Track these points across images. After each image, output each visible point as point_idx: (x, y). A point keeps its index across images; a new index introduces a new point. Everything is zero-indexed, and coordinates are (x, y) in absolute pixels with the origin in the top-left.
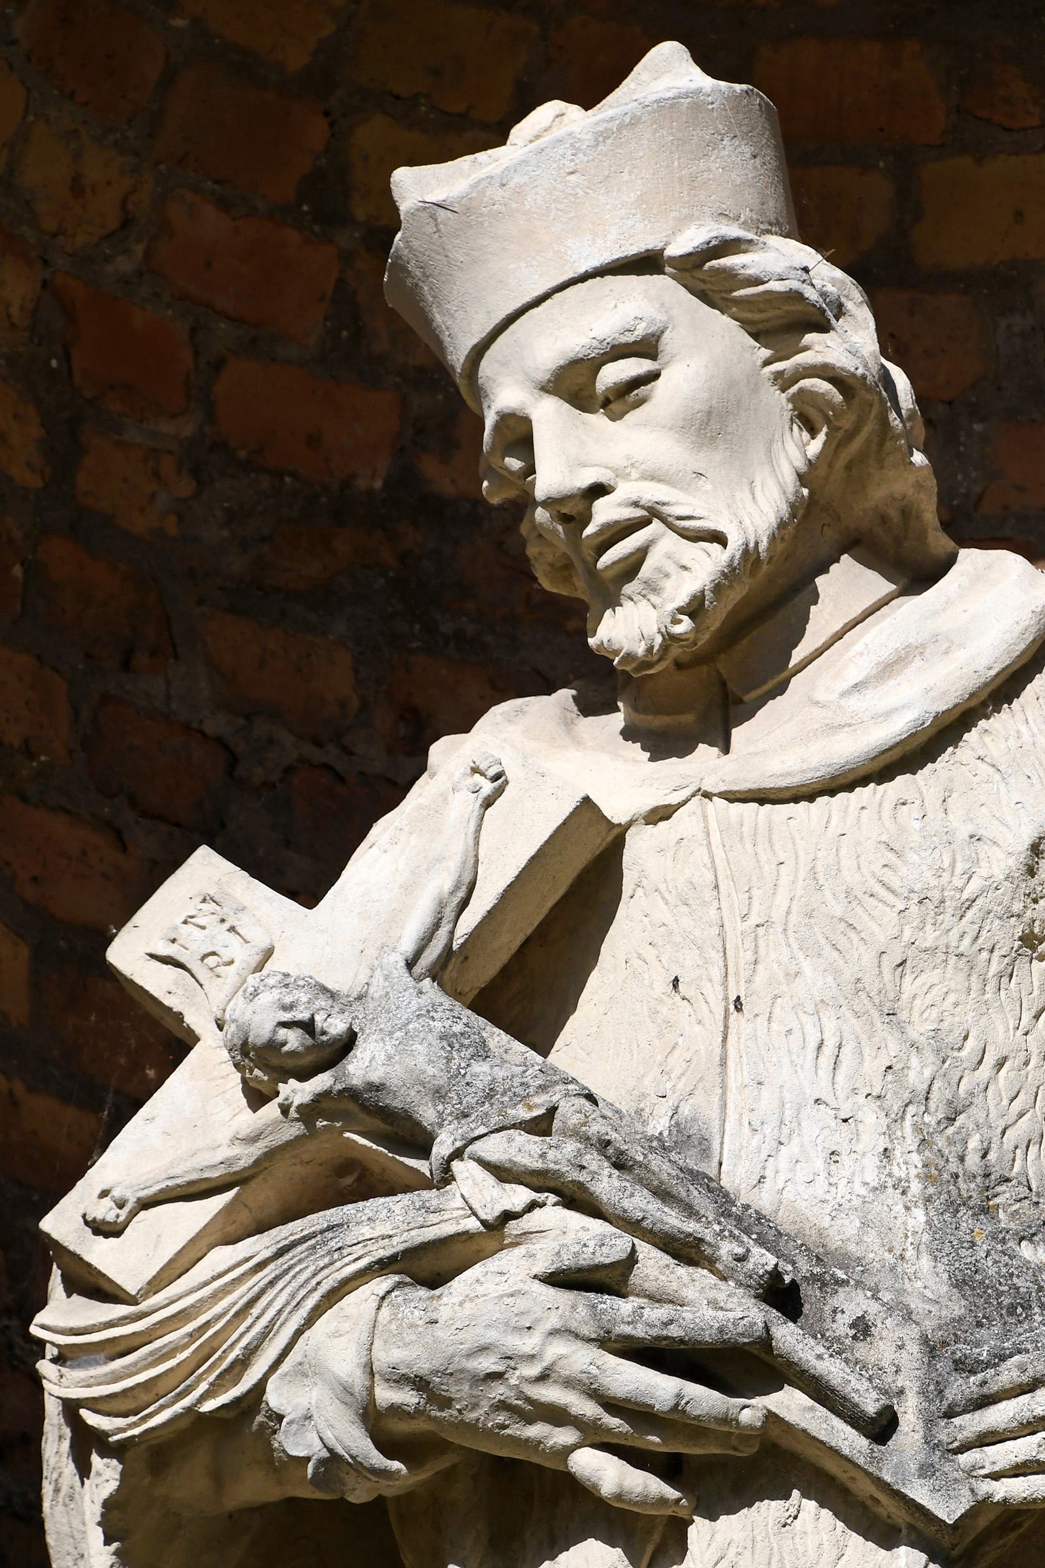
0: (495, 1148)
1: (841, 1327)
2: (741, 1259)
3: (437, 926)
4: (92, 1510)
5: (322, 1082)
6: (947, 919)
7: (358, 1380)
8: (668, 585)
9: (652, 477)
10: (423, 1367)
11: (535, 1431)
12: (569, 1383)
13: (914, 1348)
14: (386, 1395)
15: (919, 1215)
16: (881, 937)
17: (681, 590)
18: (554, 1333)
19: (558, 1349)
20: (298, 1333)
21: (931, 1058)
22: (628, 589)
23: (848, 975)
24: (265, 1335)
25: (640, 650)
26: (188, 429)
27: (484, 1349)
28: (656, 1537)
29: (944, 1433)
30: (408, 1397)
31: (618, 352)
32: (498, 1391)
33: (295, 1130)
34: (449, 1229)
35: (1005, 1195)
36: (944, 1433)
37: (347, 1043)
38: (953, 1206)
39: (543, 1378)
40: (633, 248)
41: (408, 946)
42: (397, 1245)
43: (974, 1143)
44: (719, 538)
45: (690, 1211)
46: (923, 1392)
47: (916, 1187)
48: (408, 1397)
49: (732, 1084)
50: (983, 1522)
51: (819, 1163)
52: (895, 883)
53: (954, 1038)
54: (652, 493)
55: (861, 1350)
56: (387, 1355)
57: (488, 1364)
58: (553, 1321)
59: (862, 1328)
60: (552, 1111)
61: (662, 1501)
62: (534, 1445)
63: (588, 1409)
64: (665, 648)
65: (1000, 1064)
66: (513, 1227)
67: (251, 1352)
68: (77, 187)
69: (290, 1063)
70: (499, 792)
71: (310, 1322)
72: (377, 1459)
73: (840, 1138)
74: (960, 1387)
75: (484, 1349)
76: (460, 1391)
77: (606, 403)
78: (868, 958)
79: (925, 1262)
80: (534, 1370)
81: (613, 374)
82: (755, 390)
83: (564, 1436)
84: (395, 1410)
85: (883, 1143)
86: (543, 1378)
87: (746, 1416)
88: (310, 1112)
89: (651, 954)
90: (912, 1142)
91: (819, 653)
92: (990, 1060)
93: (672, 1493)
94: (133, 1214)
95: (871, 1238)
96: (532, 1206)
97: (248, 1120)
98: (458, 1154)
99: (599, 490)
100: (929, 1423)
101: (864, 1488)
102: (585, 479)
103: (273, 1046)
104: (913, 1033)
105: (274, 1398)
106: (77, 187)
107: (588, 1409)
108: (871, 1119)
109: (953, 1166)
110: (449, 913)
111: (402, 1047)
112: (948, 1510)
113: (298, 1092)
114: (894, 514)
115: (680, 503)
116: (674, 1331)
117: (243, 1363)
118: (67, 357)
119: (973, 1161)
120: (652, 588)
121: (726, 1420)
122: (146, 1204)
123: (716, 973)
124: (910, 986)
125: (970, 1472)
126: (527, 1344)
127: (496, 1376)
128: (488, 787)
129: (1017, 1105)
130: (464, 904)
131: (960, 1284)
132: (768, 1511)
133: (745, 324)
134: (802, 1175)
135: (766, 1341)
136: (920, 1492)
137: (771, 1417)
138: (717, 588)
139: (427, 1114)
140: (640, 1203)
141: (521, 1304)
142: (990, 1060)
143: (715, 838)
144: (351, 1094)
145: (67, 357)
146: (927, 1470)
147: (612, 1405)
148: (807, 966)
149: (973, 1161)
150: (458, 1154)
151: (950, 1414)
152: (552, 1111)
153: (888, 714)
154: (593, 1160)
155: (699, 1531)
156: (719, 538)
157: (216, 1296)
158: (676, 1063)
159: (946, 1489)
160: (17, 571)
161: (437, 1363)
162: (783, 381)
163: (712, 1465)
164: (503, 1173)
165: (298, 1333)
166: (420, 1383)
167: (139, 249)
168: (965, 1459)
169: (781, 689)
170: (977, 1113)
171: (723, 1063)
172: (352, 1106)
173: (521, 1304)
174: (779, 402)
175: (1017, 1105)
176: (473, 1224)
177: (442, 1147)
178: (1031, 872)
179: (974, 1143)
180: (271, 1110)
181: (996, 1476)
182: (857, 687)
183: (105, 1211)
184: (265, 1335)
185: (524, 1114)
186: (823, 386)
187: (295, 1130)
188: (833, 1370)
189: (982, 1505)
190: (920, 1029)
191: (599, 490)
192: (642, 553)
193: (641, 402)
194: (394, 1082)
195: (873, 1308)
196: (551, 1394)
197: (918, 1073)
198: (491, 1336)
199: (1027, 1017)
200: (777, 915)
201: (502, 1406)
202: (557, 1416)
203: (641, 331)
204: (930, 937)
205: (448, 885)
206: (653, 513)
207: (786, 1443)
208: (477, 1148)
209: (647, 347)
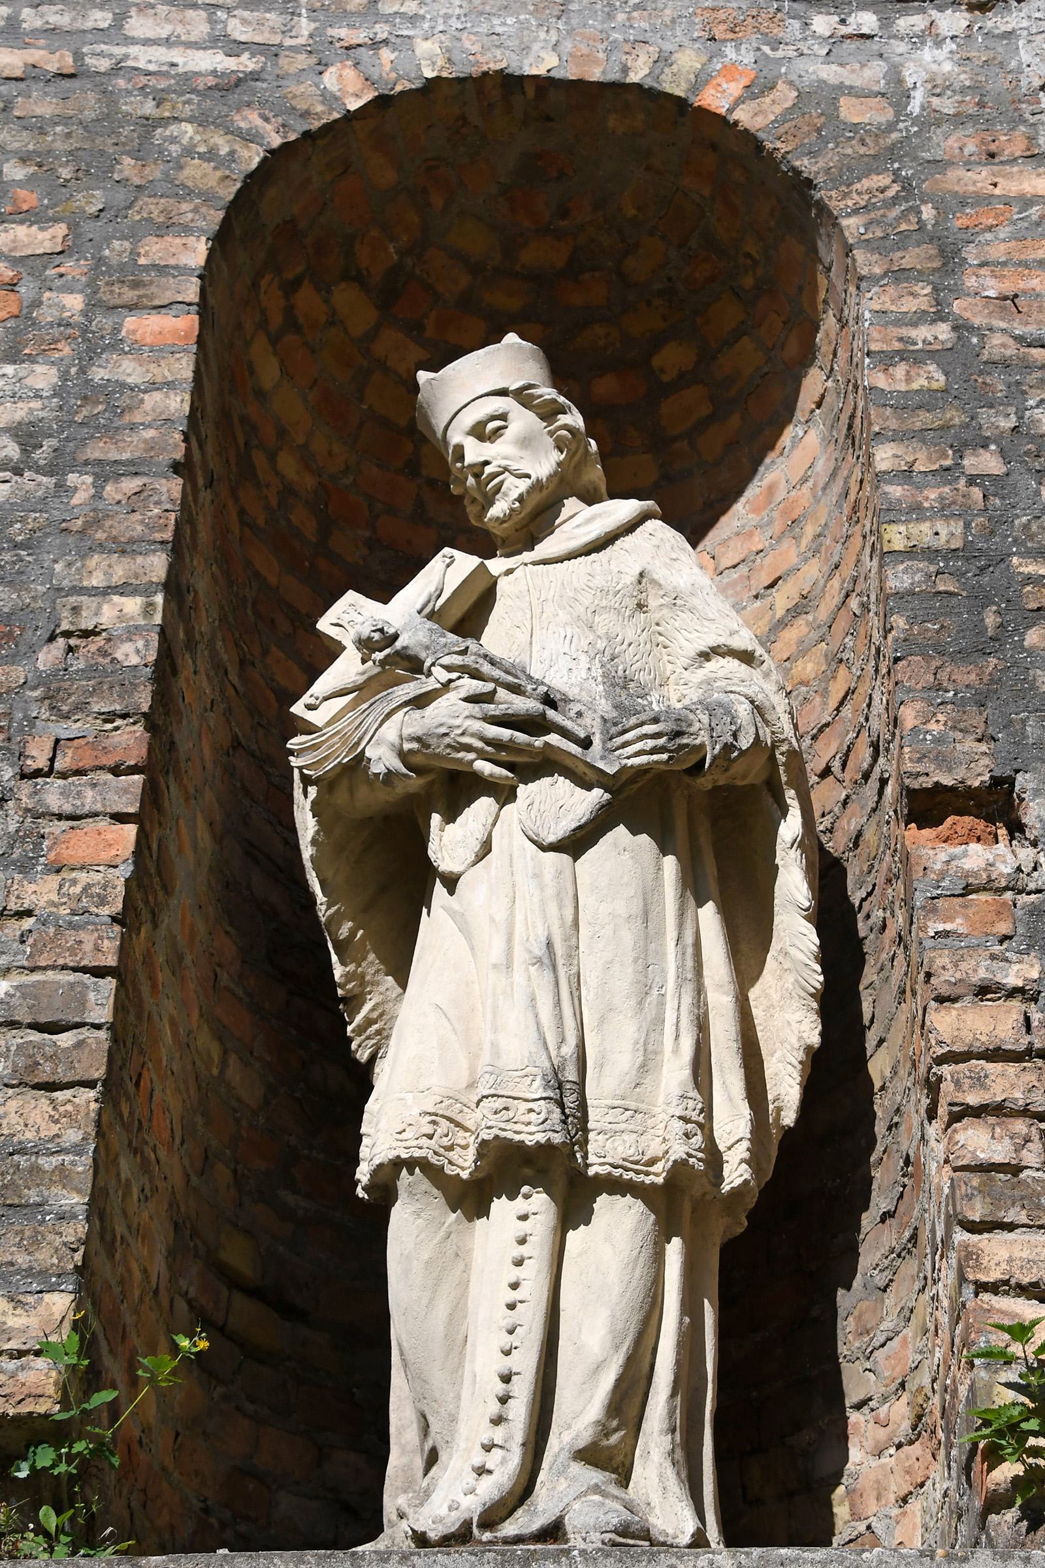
0: (446, 660)
1: (572, 714)
2: (535, 690)
3: (429, 601)
4: (308, 806)
5: (387, 651)
6: (610, 597)
7: (397, 741)
8: (511, 493)
9: (505, 458)
10: (420, 733)
11: (461, 755)
12: (472, 735)
13: (599, 720)
14: (407, 746)
15: (601, 687)
16: (587, 603)
17: (515, 494)
18: (467, 717)
19: (468, 722)
20: (377, 730)
21: (604, 640)
22: (497, 497)
23: (575, 615)
24: (365, 733)
25: (501, 515)
26: (367, 534)
27: (441, 725)
28: (506, 794)
29: (609, 744)
30: (415, 746)
31: (493, 418)
32: (447, 740)
33: (378, 669)
34: (430, 688)
35: (632, 685)
36: (609, 744)
37: (396, 637)
38: (613, 685)
39: (463, 734)
40: (498, 387)
41: (418, 607)
42: (411, 695)
43: (621, 667)
44: (528, 476)
45: (516, 677)
46: (602, 733)
47: (600, 679)
48: (415, 746)
49: (534, 650)
50: (624, 777)
51: (565, 672)
52: (592, 585)
53: (614, 635)
54: (504, 463)
55: (579, 721)
56: (407, 731)
57: (443, 730)
58: (467, 713)
59: (579, 714)
60: (467, 648)
61: (507, 778)
62: (460, 761)
63: (479, 744)
64: (510, 515)
65: (630, 645)
66: (453, 685)
67: (360, 739)
68: (330, 453)
69: (376, 646)
70: (452, 562)
71: (380, 725)
72: (405, 771)
73: (572, 665)
74: (614, 730)
75: (441, 725)
76: (433, 741)
77: (489, 438)
78: (582, 609)
79: (603, 701)
80: (460, 731)
81: (492, 425)
82: (541, 435)
83: (472, 756)
84: (410, 751)
85: (588, 666)
86: (463, 734)
87: (537, 744)
88: (383, 663)
89: (506, 616)
90: (598, 665)
91: (565, 522)
92: (626, 643)
93: (511, 775)
94: (321, 702)
95: (583, 693)
96: (459, 678)
97: (362, 668)
98: (433, 664)
99: (487, 463)
100: (604, 742)
101: (581, 769)
102: (482, 459)
103: (369, 639)
104: (598, 633)
105: (367, 754)
106: (330, 453)
107: (479, 744)
108: (584, 658)
109: (613, 674)
110: (433, 598)
111: (415, 634)
112: (611, 770)
113: (378, 656)
114: (592, 490)
115: (514, 466)
116: (510, 711)
117: (358, 743)
118: (326, 505)
119: (620, 673)
120: (506, 495)
121: (529, 745)
122: (326, 699)
123: (529, 616)
124: (597, 619)
125: (619, 757)
126: (457, 722)
127: (446, 735)
128: (448, 561)
129: (636, 658)
130: (439, 596)
131: (616, 707)
132: (546, 781)
133: (538, 414)
134: (558, 675)
135: (543, 715)
136: (601, 765)
137: (546, 743)
138: (528, 492)
139: (423, 655)
140: (497, 673)
141: (455, 708)
142: (626, 643)
143: (529, 577)
144: (397, 653)
145: (326, 505)
146: (603, 758)
147: (489, 742)
148: (560, 612)
149: (620, 673)
150: (433, 664)
151: (610, 739)
152: (467, 648)
153: (589, 533)
154: (481, 661)
155: (522, 790)
156: (528, 476)
157: (349, 725)
158: (515, 647)
159: (611, 763)
160: (307, 564)
161: (425, 731)
162: (551, 434)
163: (526, 766)
164: (449, 668)
165: (377, 730)
166: (418, 739)
167: (352, 478)
168: (617, 753)
169: (552, 533)
170: (622, 659)
171: (531, 643)
172: (398, 659)
173: (455, 708)
174: (550, 441)
175: (636, 658)
176: (439, 686)
177: (427, 664)
178: (640, 583)
179: (621, 667)
180: (370, 663)
181: (628, 758)
182: (578, 526)
183: (312, 701)
184: (365, 733)
185: (457, 649)
186: (564, 432)
187: (378, 669)
188: (568, 724)
189: (624, 768)
190: (601, 631)
191: (487, 463)
192: (502, 483)
193: (501, 435)
194: (411, 645)
195: (584, 708)
196: (466, 740)
197: (601, 645)
198: (444, 720)
199: (639, 631)
200: (550, 597)
201: (449, 746)
202: (468, 748)
203: (501, 411)
204: (604, 603)
205: (433, 589)
206: (506, 469)
207: (554, 757)
208: (441, 661)
209: (503, 417)
